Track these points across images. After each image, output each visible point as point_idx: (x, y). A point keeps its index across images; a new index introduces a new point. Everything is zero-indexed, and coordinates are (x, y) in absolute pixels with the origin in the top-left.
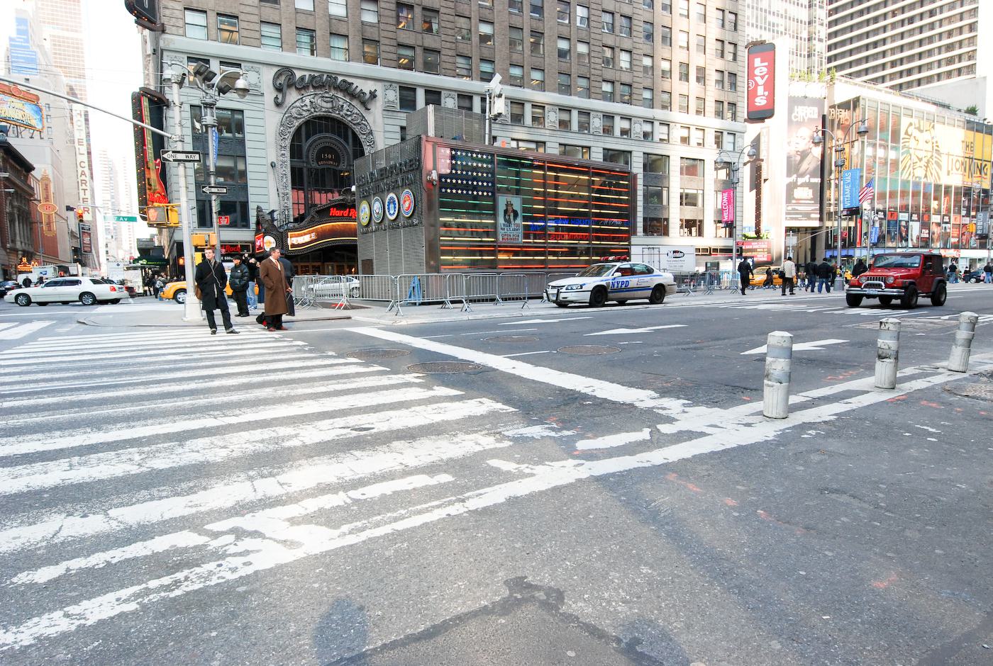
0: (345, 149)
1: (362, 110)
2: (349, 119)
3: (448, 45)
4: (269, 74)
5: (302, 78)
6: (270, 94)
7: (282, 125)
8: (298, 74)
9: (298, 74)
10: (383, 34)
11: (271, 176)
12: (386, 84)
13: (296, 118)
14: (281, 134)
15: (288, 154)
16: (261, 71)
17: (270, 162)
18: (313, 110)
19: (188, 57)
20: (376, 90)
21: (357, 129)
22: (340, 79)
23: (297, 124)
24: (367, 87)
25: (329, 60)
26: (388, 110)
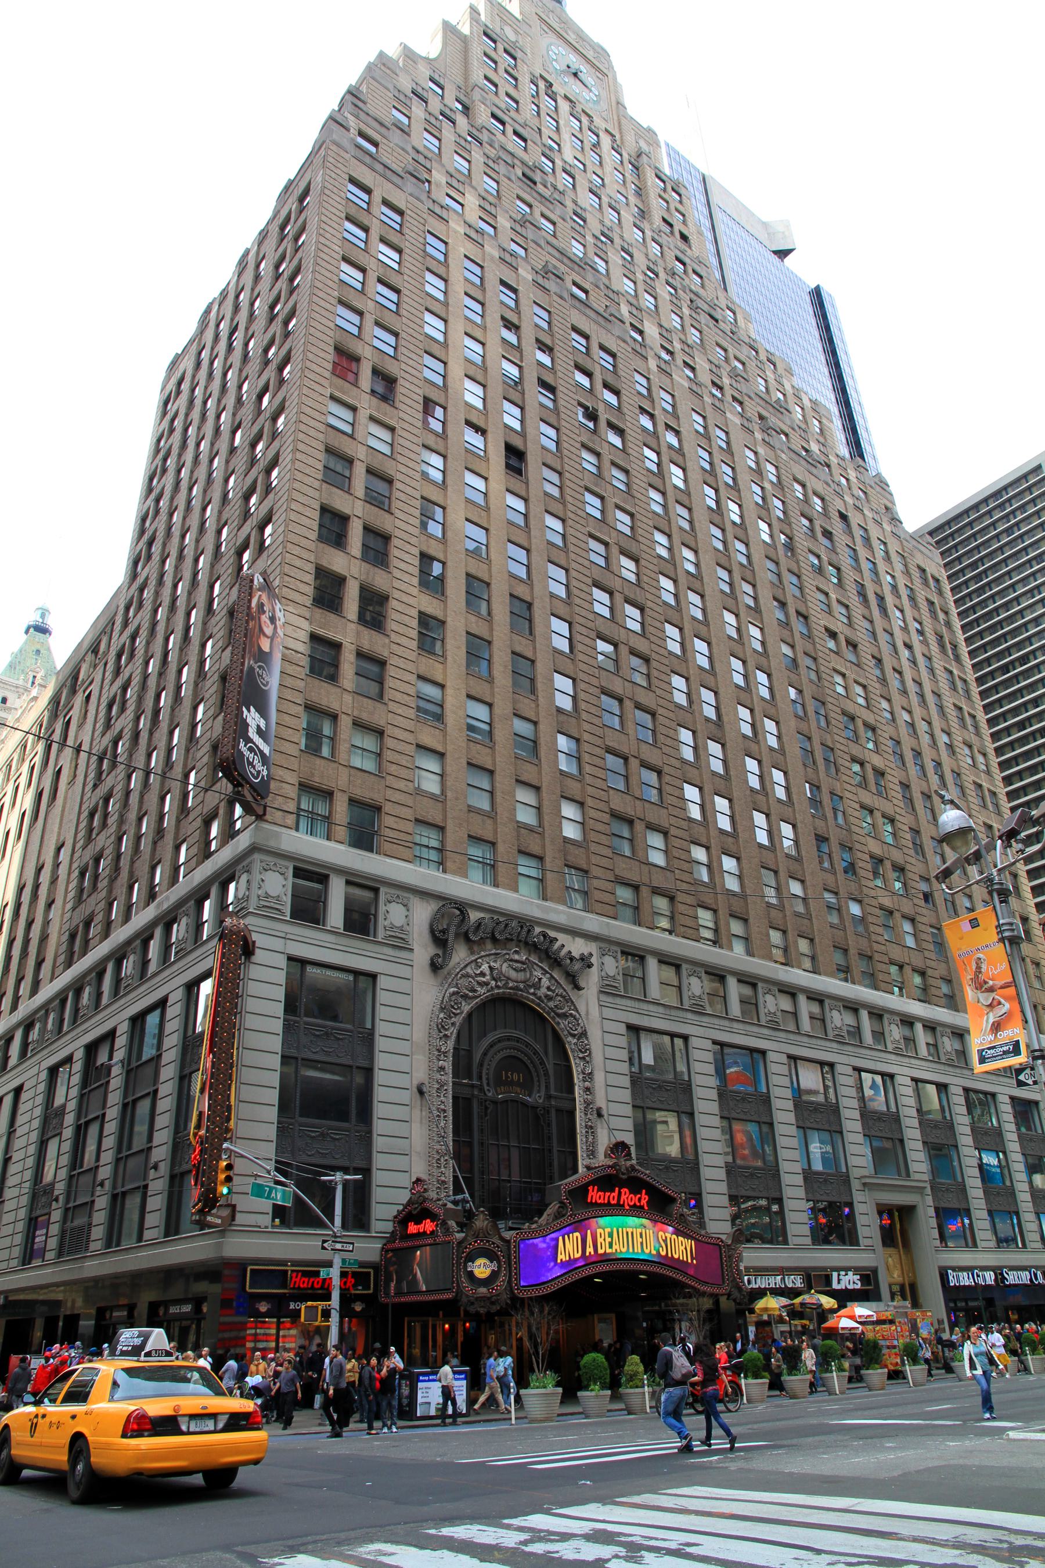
0: (542, 1063)
1: (569, 988)
2: (551, 1004)
3: (685, 886)
4: (422, 913)
5: (479, 925)
6: (423, 951)
7: (442, 1009)
8: (474, 916)
9: (474, 916)
10: (595, 859)
11: (417, 1113)
12: (603, 945)
13: (465, 997)
14: (441, 1027)
15: (448, 1065)
16: (410, 905)
17: (415, 1083)
18: (493, 983)
19: (295, 868)
20: (591, 955)
21: (563, 1025)
22: (538, 930)
23: (466, 1008)
24: (577, 947)
25: (515, 895)
26: (607, 990)
